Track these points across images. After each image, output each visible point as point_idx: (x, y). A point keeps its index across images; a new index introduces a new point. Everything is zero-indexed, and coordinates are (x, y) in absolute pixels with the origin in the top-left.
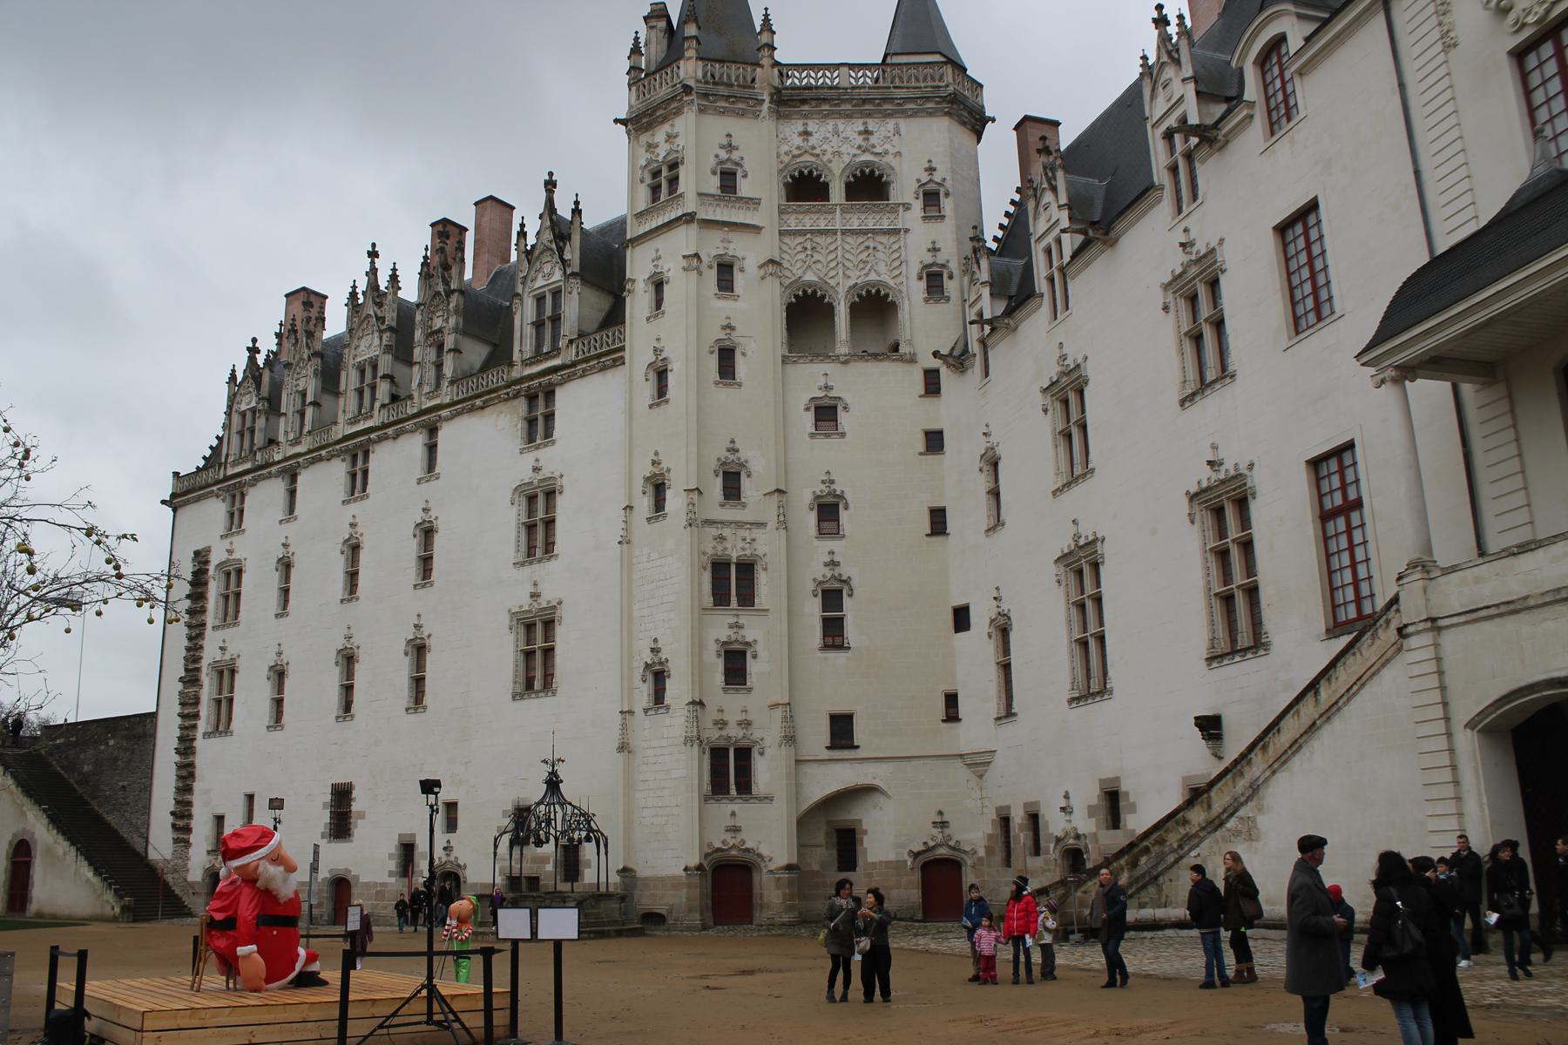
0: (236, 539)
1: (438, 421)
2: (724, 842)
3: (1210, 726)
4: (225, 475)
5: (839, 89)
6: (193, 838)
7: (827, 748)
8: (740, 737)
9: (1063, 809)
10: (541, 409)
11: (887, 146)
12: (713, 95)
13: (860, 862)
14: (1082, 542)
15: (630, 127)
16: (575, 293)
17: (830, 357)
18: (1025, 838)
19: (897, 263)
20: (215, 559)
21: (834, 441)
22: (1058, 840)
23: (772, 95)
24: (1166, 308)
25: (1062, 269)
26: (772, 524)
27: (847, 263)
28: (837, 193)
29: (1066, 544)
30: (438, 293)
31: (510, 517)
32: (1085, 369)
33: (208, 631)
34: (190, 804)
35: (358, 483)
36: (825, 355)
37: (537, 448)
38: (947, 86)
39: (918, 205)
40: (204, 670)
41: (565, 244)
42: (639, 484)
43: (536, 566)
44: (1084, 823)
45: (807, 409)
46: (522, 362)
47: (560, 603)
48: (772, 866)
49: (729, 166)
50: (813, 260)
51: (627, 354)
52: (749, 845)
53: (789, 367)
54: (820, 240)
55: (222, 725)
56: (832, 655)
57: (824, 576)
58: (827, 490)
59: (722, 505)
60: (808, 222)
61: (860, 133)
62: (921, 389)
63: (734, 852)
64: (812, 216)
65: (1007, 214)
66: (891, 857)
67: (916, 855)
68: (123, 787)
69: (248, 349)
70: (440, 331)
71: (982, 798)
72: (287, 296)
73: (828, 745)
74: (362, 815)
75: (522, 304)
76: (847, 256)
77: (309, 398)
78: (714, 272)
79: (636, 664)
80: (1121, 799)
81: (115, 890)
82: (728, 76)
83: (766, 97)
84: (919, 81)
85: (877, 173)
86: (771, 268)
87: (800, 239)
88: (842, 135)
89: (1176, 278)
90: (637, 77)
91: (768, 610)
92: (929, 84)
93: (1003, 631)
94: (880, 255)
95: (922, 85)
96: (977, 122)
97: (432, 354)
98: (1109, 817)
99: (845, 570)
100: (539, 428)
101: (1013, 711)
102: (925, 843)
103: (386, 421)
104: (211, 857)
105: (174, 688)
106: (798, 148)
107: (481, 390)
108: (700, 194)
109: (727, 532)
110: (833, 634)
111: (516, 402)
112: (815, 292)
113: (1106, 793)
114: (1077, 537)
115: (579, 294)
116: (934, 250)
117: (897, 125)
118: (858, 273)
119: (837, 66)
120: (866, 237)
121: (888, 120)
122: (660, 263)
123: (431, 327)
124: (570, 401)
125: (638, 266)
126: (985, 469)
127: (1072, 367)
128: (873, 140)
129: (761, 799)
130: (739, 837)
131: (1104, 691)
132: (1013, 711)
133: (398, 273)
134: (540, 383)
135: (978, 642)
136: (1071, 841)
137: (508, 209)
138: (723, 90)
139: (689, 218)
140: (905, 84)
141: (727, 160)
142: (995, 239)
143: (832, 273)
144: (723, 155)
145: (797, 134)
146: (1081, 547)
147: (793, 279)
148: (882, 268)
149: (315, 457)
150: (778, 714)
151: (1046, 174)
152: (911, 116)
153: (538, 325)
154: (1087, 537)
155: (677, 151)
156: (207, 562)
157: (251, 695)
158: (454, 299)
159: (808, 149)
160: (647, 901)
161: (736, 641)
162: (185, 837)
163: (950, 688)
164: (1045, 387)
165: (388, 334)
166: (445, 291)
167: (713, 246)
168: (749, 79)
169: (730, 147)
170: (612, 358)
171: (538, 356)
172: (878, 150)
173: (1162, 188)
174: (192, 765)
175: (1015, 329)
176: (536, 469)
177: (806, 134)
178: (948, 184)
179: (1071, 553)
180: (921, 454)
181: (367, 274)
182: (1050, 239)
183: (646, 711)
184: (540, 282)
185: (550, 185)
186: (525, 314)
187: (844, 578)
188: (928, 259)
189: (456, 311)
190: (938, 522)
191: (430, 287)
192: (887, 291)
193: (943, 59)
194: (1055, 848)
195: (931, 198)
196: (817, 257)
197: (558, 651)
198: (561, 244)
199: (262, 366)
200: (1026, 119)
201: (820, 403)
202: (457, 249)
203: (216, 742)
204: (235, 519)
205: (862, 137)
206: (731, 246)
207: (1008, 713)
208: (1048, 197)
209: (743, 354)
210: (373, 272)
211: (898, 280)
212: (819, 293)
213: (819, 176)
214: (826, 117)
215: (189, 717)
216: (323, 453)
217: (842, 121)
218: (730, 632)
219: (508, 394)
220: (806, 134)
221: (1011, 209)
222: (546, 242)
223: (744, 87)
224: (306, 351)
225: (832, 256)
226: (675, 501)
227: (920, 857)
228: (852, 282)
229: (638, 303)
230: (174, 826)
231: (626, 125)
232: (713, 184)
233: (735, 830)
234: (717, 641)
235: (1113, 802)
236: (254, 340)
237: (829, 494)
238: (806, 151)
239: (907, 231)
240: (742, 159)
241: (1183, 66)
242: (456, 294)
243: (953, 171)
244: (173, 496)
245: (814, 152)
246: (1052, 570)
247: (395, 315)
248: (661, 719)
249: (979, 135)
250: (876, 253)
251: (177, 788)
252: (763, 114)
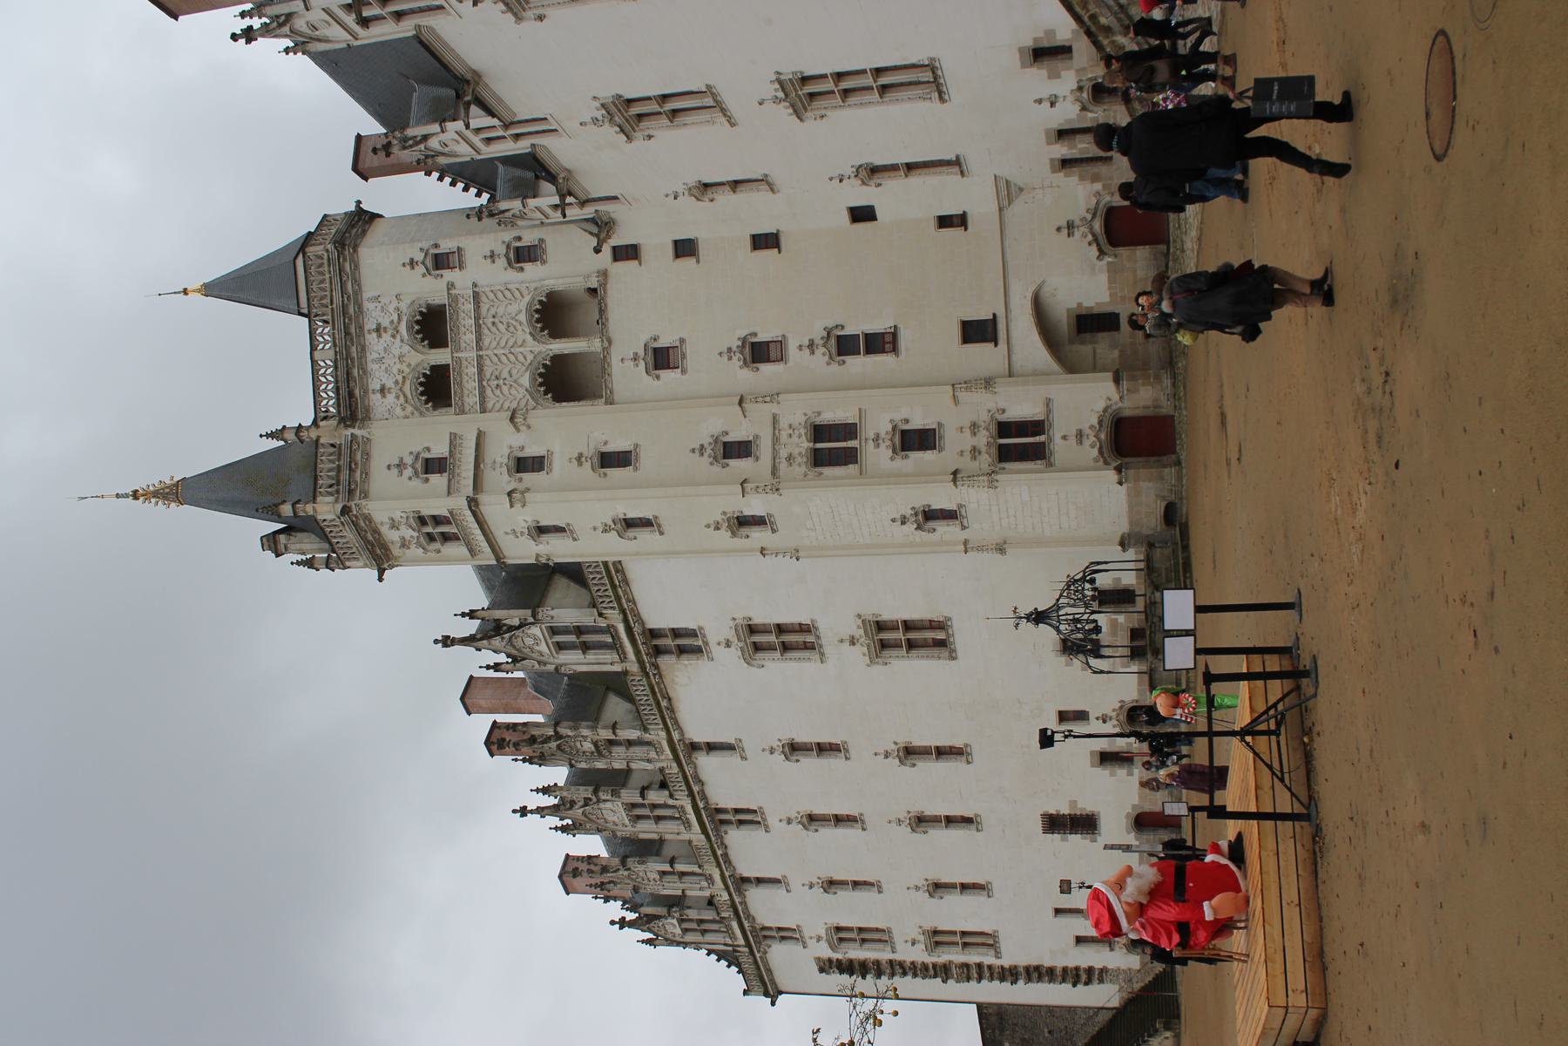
0: (807, 934)
1: (684, 743)
2: (1092, 446)
4: (745, 947)
5: (336, 359)
6: (1098, 965)
7: (996, 345)
8: (987, 433)
9: (1052, 104)
10: (669, 642)
11: (391, 309)
12: (349, 485)
13: (1110, 309)
14: (781, 95)
15: (386, 566)
16: (552, 613)
17: (605, 357)
18: (1081, 142)
19: (508, 293)
20: (826, 952)
21: (689, 349)
22: (1084, 108)
23: (347, 426)
24: (541, 18)
25: (506, 126)
26: (772, 407)
27: (510, 344)
28: (440, 356)
29: (784, 111)
30: (559, 747)
31: (778, 670)
32: (606, 98)
33: (898, 957)
34: (1065, 970)
35: (747, 818)
36: (604, 361)
37: (706, 644)
38: (327, 251)
39: (448, 275)
40: (934, 959)
41: (505, 625)
42: (738, 542)
43: (824, 641)
44: (1066, 82)
45: (658, 377)
46: (622, 662)
47: (859, 616)
48: (1116, 397)
49: (419, 466)
50: (508, 377)
51: (610, 559)
52: (1095, 421)
53: (617, 397)
54: (488, 372)
55: (988, 940)
56: (903, 343)
57: (824, 354)
58: (738, 355)
59: (757, 459)
60: (471, 384)
61: (379, 336)
62: (633, 264)
63: (1103, 436)
64: (464, 381)
65: (453, 184)
66: (1103, 278)
67: (1102, 253)
68: (1050, 1032)
69: (621, 928)
70: (595, 744)
71: (1043, 188)
72: (568, 894)
73: (992, 345)
74: (1073, 803)
75: (566, 665)
76: (502, 344)
77: (667, 868)
78: (525, 476)
79: (918, 540)
80: (1041, 46)
81: (1150, 1036)
82: (330, 470)
83: (349, 431)
84: (325, 280)
85: (418, 317)
86: (519, 420)
87: (489, 392)
88: (383, 355)
89: (509, 8)
90: (336, 561)
91: (860, 409)
92: (326, 269)
93: (874, 171)
94: (501, 311)
95: (328, 276)
96: (362, 219)
97: (619, 751)
98: (1060, 57)
99: (818, 333)
100: (687, 643)
101: (954, 159)
102: (1090, 244)
103: (686, 793)
104: (1117, 947)
105: (953, 988)
106: (398, 397)
107: (652, 701)
108: (449, 493)
109: (784, 453)
110: (880, 343)
111: (663, 667)
112: (541, 375)
113: (1034, 62)
114: (776, 100)
115: (553, 609)
116: (492, 256)
117: (369, 300)
118: (520, 332)
119: (313, 361)
120: (483, 326)
121: (365, 309)
122: (518, 530)
123: (592, 753)
124: (659, 613)
125: (522, 551)
126: (711, 196)
127: (604, 112)
128: (385, 323)
129: (1049, 411)
130: (1087, 431)
131: (932, 67)
132: (954, 159)
133: (541, 787)
134: (643, 643)
135: (886, 197)
136: (1085, 95)
137: (473, 682)
138: (345, 475)
139: (473, 503)
140: (328, 293)
141: (413, 467)
142: (478, 195)
143: (521, 358)
144: (409, 472)
145: (384, 400)
146: (786, 95)
147: (528, 396)
148: (513, 308)
149: (724, 861)
150: (963, 395)
151: (411, 146)
152: (359, 285)
153: (585, 647)
154: (776, 90)
155: (407, 517)
156: (830, 960)
157: (958, 913)
158: (563, 731)
159: (398, 388)
160: (1153, 521)
161: (891, 440)
162: (1097, 972)
163: (933, 223)
164: (626, 138)
165: (601, 794)
166: (556, 740)
167: (499, 478)
168: (332, 450)
169: (401, 466)
170: (615, 573)
171: (616, 646)
172: (395, 317)
173: (418, 27)
174: (1027, 969)
175: (568, 171)
176: (728, 644)
177: (383, 390)
178: (425, 245)
179: (793, 106)
180: (698, 261)
181: (543, 817)
182: (476, 140)
183: (964, 528)
184: (543, 648)
185: (447, 641)
186: (575, 661)
187: (825, 334)
188: (502, 262)
189: (575, 728)
190: (765, 241)
191: (553, 755)
192: (536, 302)
193: (301, 255)
194: (1091, 112)
195: (440, 262)
196: (505, 374)
197: (906, 617)
198: (505, 628)
199: (637, 915)
200: (355, 169)
201: (651, 365)
202: (515, 731)
203: (1004, 946)
204: (786, 935)
205: (383, 334)
206: (499, 460)
207: (956, 163)
208: (434, 143)
209: (606, 443)
210: (541, 811)
211: (525, 292)
212: (542, 370)
213: (425, 375)
214: (365, 372)
215: (981, 972)
216: (719, 852)
217: (368, 354)
218: (883, 446)
219: (654, 675)
220: (383, 390)
221: (448, 180)
222: (504, 643)
223: (340, 454)
224: (621, 872)
225: (504, 359)
226: (754, 506)
227: (1103, 248)
228: (529, 338)
229: (559, 550)
230: (1086, 984)
231: (385, 569)
232: (439, 481)
233: (1080, 435)
234: (892, 459)
235: (1045, 54)
236: (613, 923)
237: (741, 353)
238: (401, 390)
239: (475, 285)
240: (411, 453)
241: (293, 9)
242: (559, 729)
243: (412, 241)
244: (766, 994)
245: (400, 382)
246: (811, 125)
247: (582, 788)
248: (971, 511)
249: (374, 217)
250: (499, 315)
251: (1050, 982)
252: (366, 435)
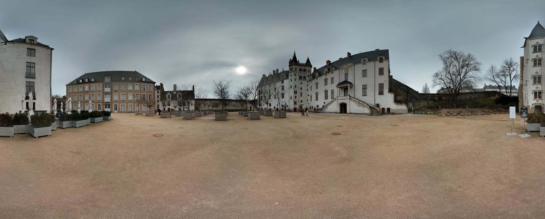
3: (324, 103)
28: (303, 71)
60: (301, 72)
93: (311, 96)
100: (283, 82)
124: (285, 81)
125: (290, 74)
135: (309, 97)
139: (293, 72)
167: (295, 73)
170: (288, 79)
190: (307, 89)
195: (309, 71)
207: (311, 101)
226: (292, 87)
235: (318, 106)
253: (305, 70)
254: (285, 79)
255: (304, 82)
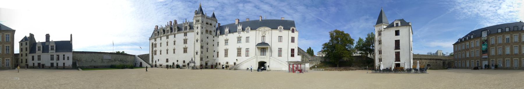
28: (209, 24)
35: (167, 38)
42: (196, 40)
55: (155, 54)
93: (218, 53)
96: (217, 23)
99: (208, 47)
105: (151, 52)
190: (213, 45)
195: (214, 26)
203: (155, 56)
215: (152, 54)
248: (197, 56)
253: (211, 24)
254: (188, 32)
255: (211, 37)
